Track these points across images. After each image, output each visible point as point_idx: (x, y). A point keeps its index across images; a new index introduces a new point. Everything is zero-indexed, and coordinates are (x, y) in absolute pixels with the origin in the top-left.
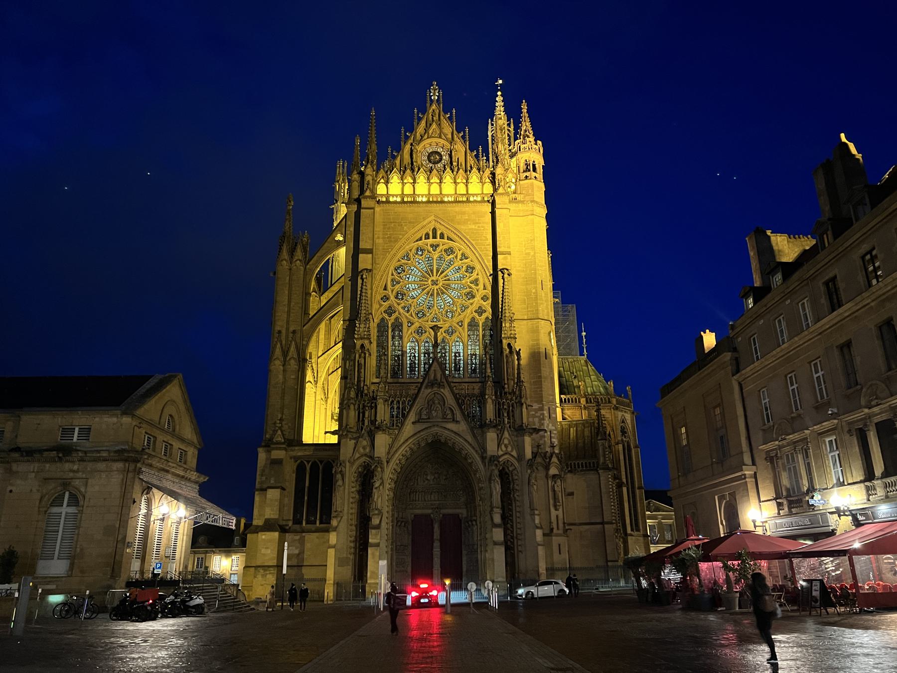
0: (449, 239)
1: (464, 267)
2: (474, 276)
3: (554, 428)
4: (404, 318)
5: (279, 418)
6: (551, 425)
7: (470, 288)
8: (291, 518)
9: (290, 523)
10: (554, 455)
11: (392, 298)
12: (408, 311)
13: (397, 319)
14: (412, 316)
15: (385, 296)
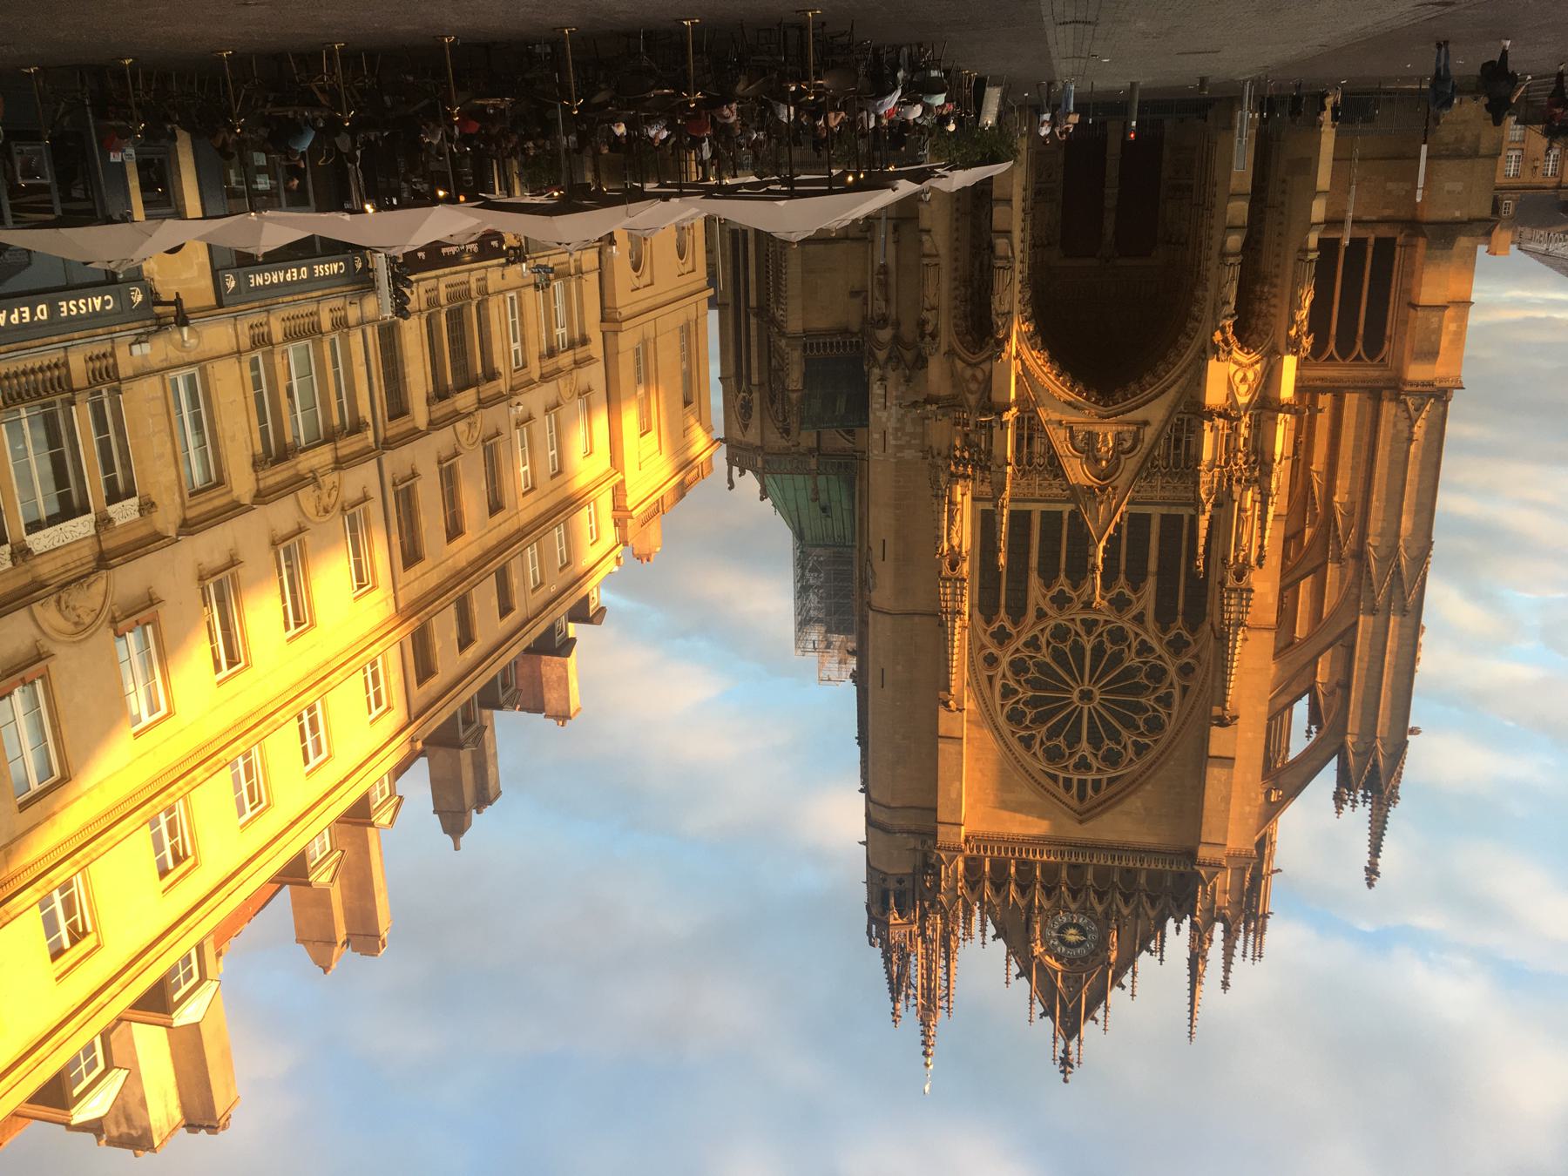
0: (1054, 778)
1: (1027, 722)
3: (878, 414)
4: (1150, 630)
5: (1414, 443)
6: (884, 419)
7: (1019, 682)
8: (1398, 249)
9: (1400, 239)
10: (881, 363)
11: (1172, 671)
12: (1143, 642)
13: (1165, 630)
14: (1137, 635)
15: (1186, 675)
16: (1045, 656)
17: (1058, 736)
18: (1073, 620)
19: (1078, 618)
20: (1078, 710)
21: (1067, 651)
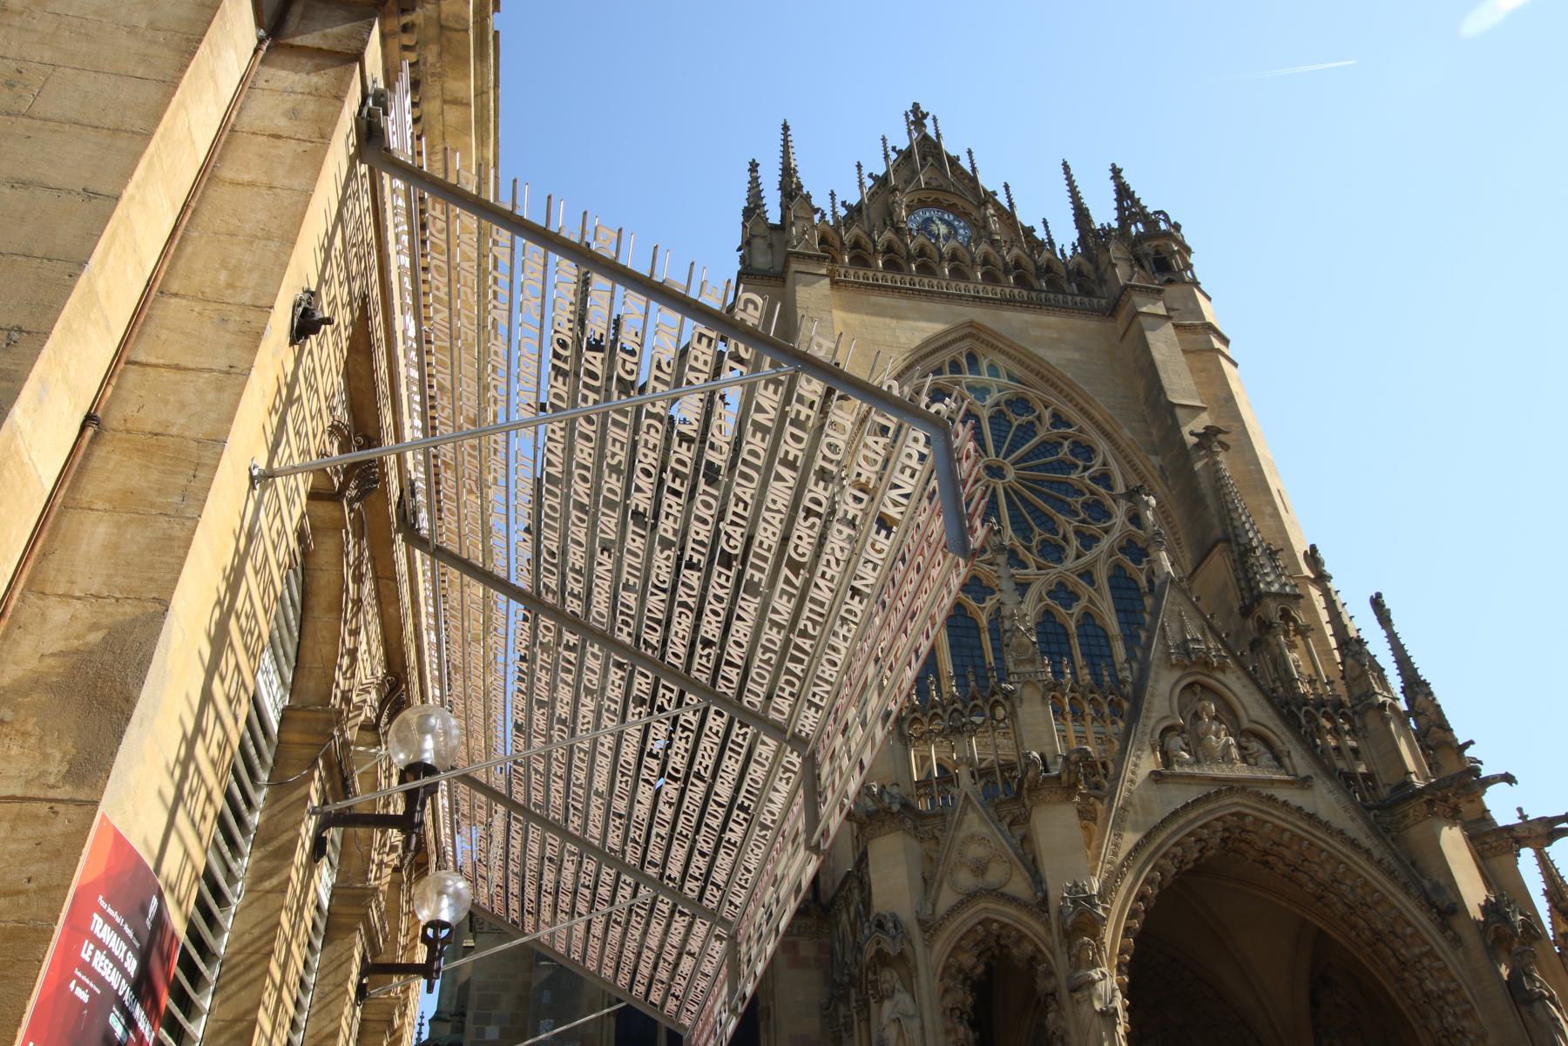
1: (1066, 444)
2: (1096, 466)
7: (1092, 493)
16: (1066, 524)
17: (1020, 426)
18: (1039, 569)
19: (1032, 570)
20: (1002, 455)
21: (1037, 530)
